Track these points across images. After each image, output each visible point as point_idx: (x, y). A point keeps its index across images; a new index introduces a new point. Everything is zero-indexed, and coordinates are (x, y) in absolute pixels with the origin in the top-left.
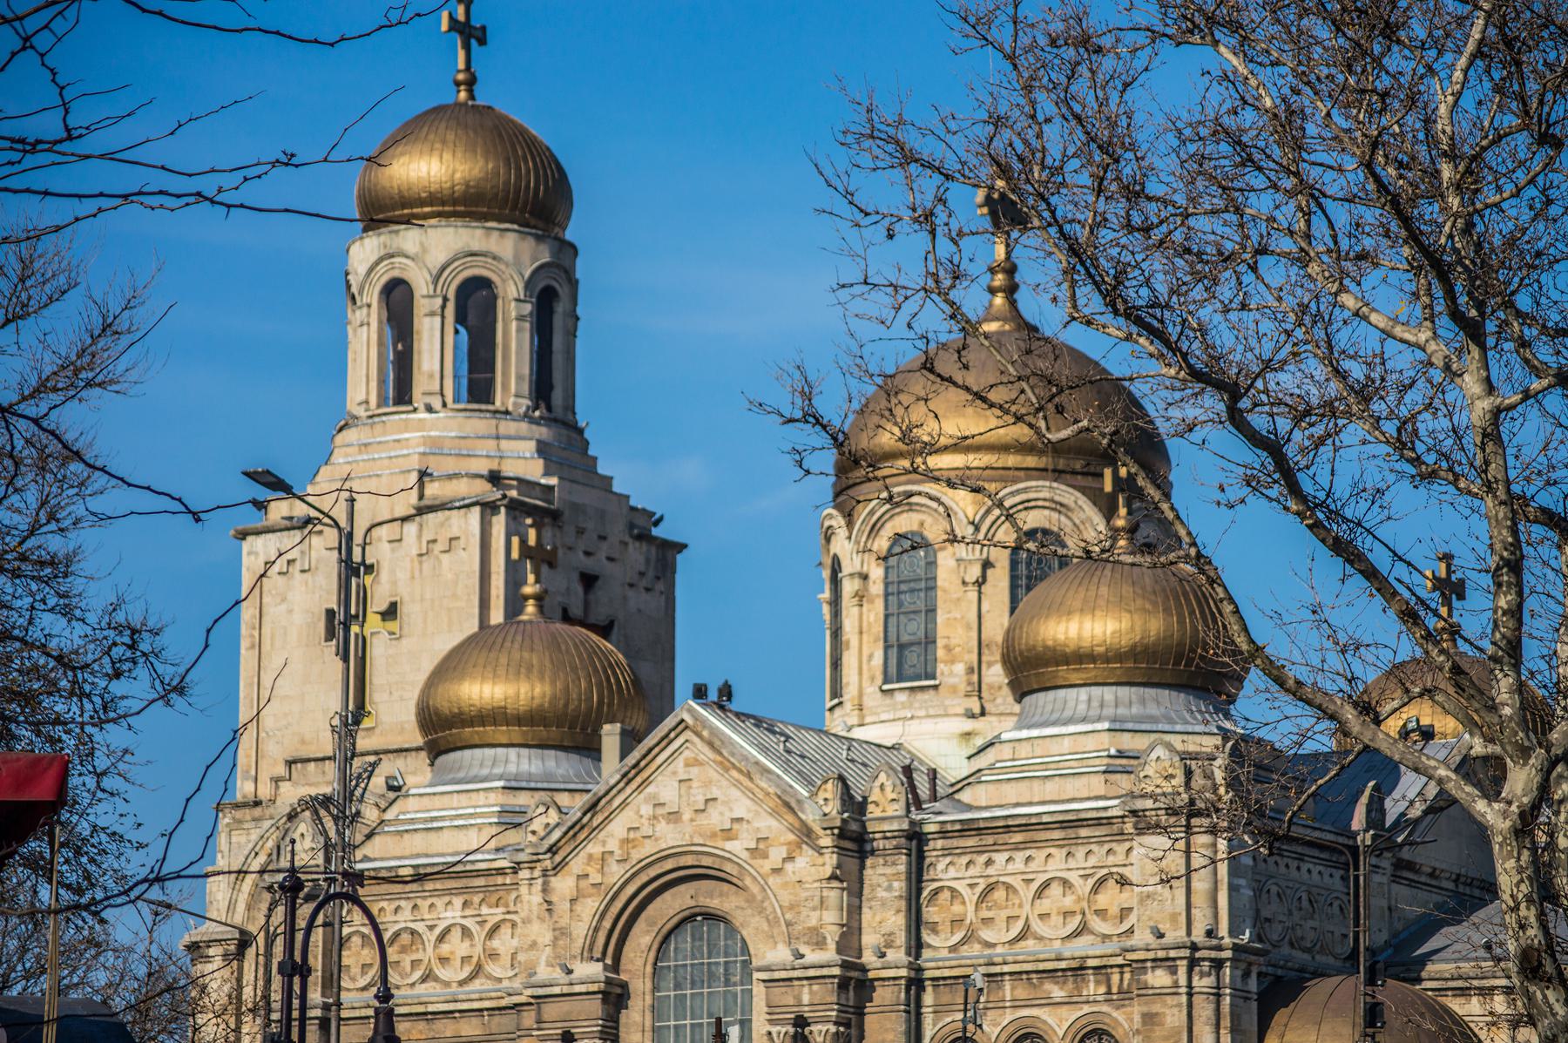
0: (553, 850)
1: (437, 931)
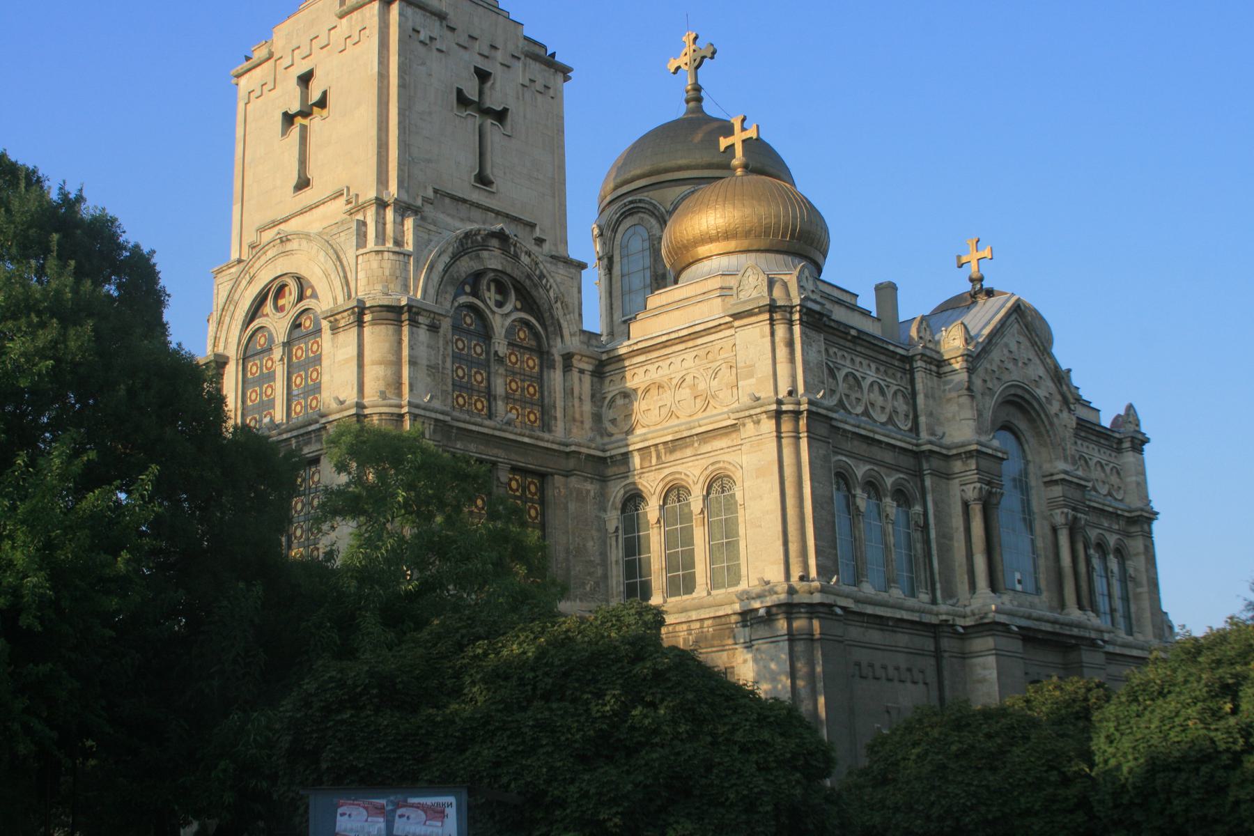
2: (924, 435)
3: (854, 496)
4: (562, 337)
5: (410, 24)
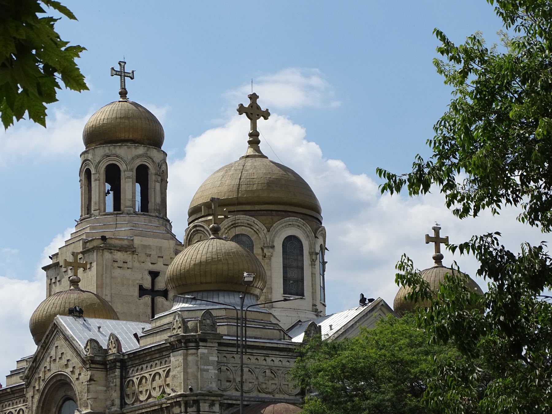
0: (27, 377)
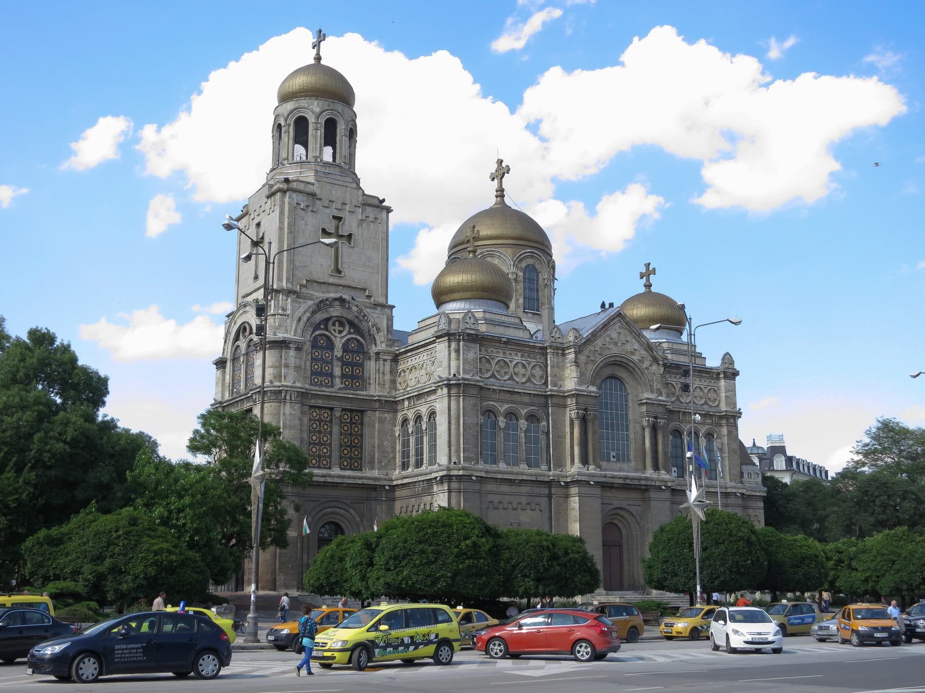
1: (514, 363)
2: (550, 387)
3: (498, 421)
4: (376, 344)
5: (295, 201)
